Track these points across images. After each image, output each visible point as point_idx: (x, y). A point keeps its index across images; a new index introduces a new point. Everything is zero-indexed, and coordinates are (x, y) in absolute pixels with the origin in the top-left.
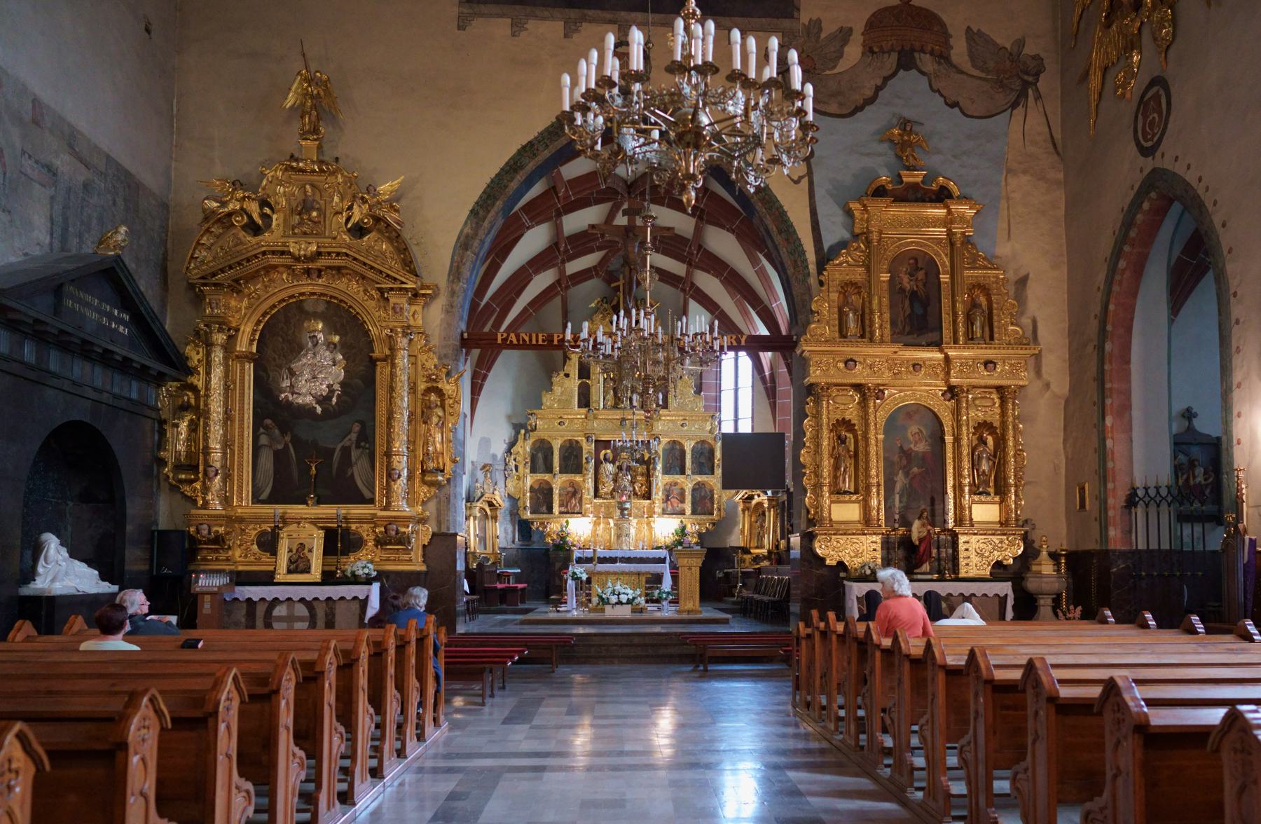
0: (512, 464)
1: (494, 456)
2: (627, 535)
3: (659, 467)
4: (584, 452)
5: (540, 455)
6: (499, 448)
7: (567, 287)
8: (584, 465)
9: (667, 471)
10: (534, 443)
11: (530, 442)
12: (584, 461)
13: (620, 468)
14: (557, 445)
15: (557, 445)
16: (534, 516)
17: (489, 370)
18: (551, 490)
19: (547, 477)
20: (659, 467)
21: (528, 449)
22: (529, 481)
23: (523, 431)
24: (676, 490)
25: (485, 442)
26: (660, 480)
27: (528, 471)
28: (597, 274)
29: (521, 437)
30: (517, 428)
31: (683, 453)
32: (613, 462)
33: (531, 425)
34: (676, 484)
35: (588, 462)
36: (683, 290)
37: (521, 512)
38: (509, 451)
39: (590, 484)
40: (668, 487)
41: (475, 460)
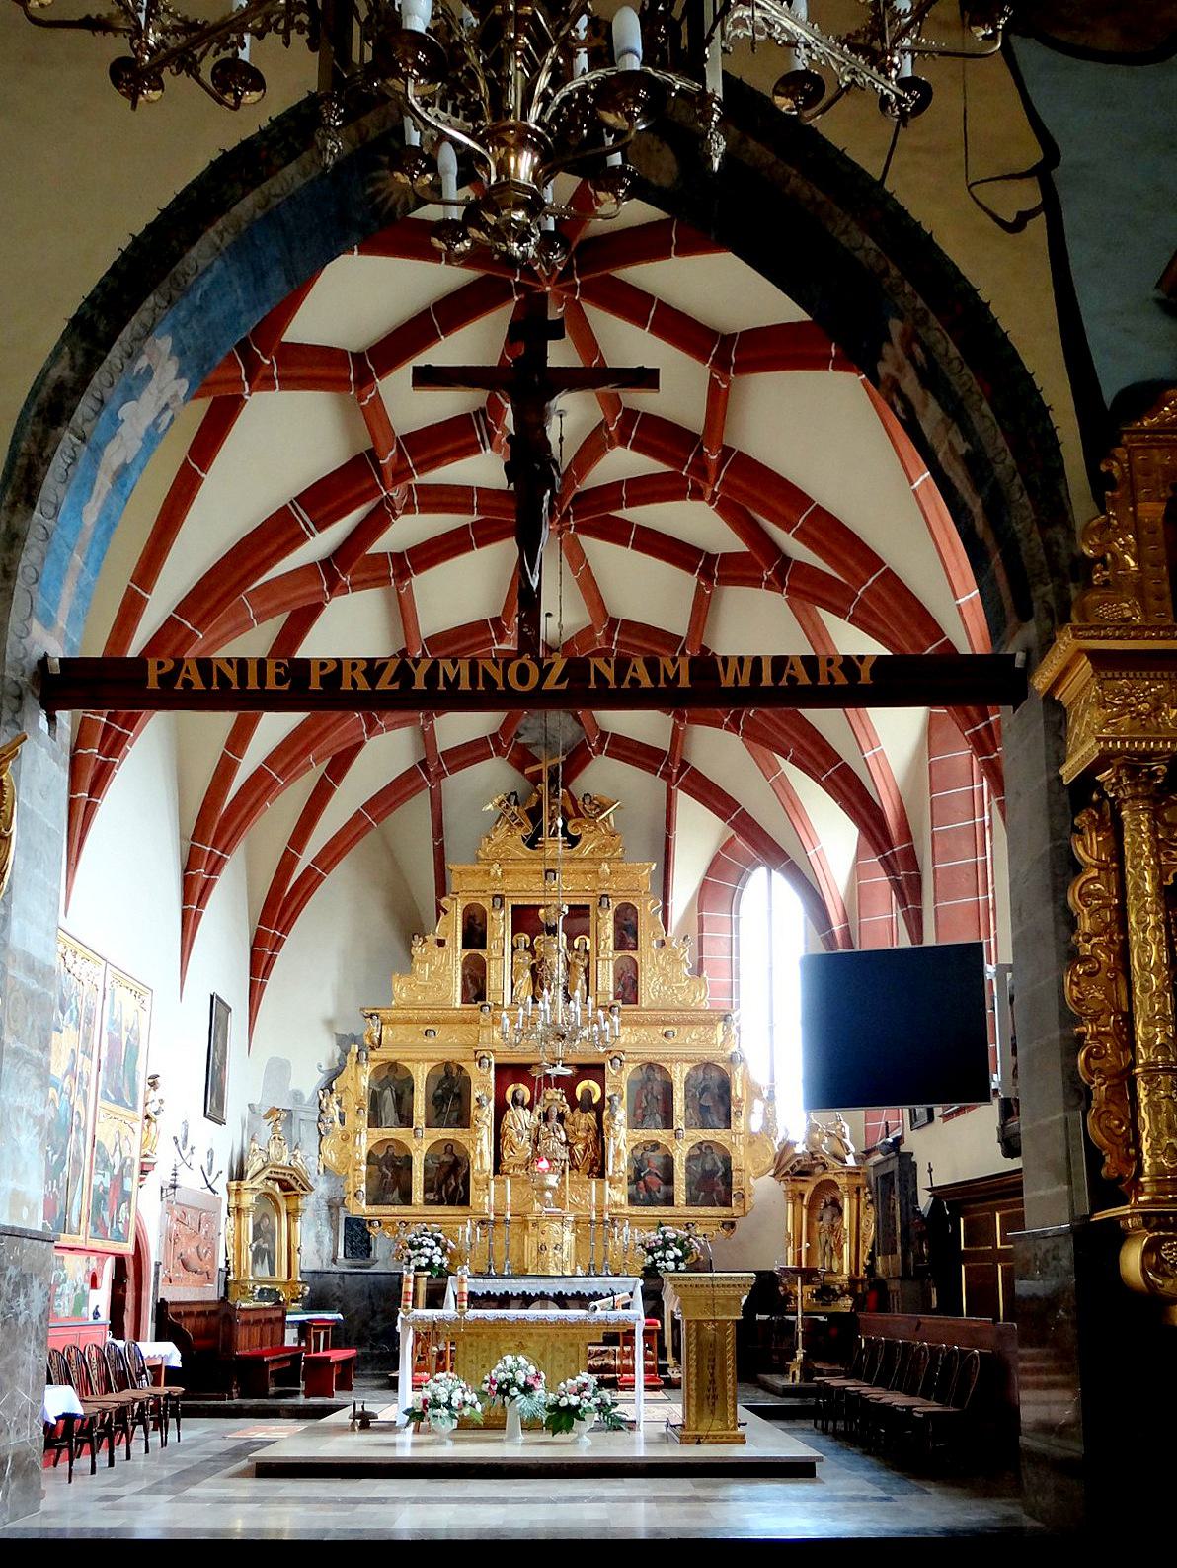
0: (334, 1110)
1: (297, 1096)
2: (558, 1247)
3: (621, 1114)
4: (474, 1086)
5: (388, 1093)
6: (307, 1081)
7: (441, 774)
8: (474, 1112)
9: (637, 1122)
10: (376, 1071)
11: (369, 1068)
12: (474, 1103)
13: (546, 1117)
14: (420, 1075)
15: (420, 1075)
16: (374, 1210)
17: (286, 930)
18: (409, 1159)
19: (401, 1134)
20: (621, 1114)
21: (365, 1082)
22: (366, 1141)
23: (355, 1049)
24: (656, 1159)
25: (279, 1069)
26: (622, 1140)
27: (364, 1122)
28: (500, 752)
29: (351, 1060)
30: (344, 1042)
31: (668, 1090)
32: (530, 1107)
33: (370, 1037)
34: (656, 1146)
35: (480, 1106)
36: (666, 775)
37: (349, 1203)
38: (328, 1087)
39: (486, 1146)
40: (638, 1153)
41: (256, 1102)
